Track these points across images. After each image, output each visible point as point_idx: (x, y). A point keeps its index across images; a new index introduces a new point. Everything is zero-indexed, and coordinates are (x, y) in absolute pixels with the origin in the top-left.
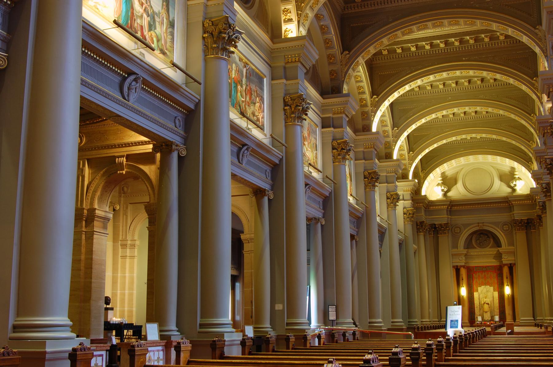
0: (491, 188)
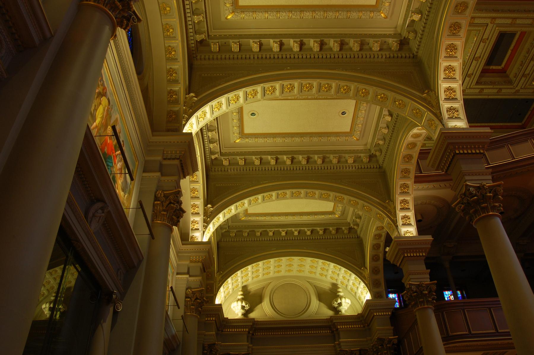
0: (308, 309)
